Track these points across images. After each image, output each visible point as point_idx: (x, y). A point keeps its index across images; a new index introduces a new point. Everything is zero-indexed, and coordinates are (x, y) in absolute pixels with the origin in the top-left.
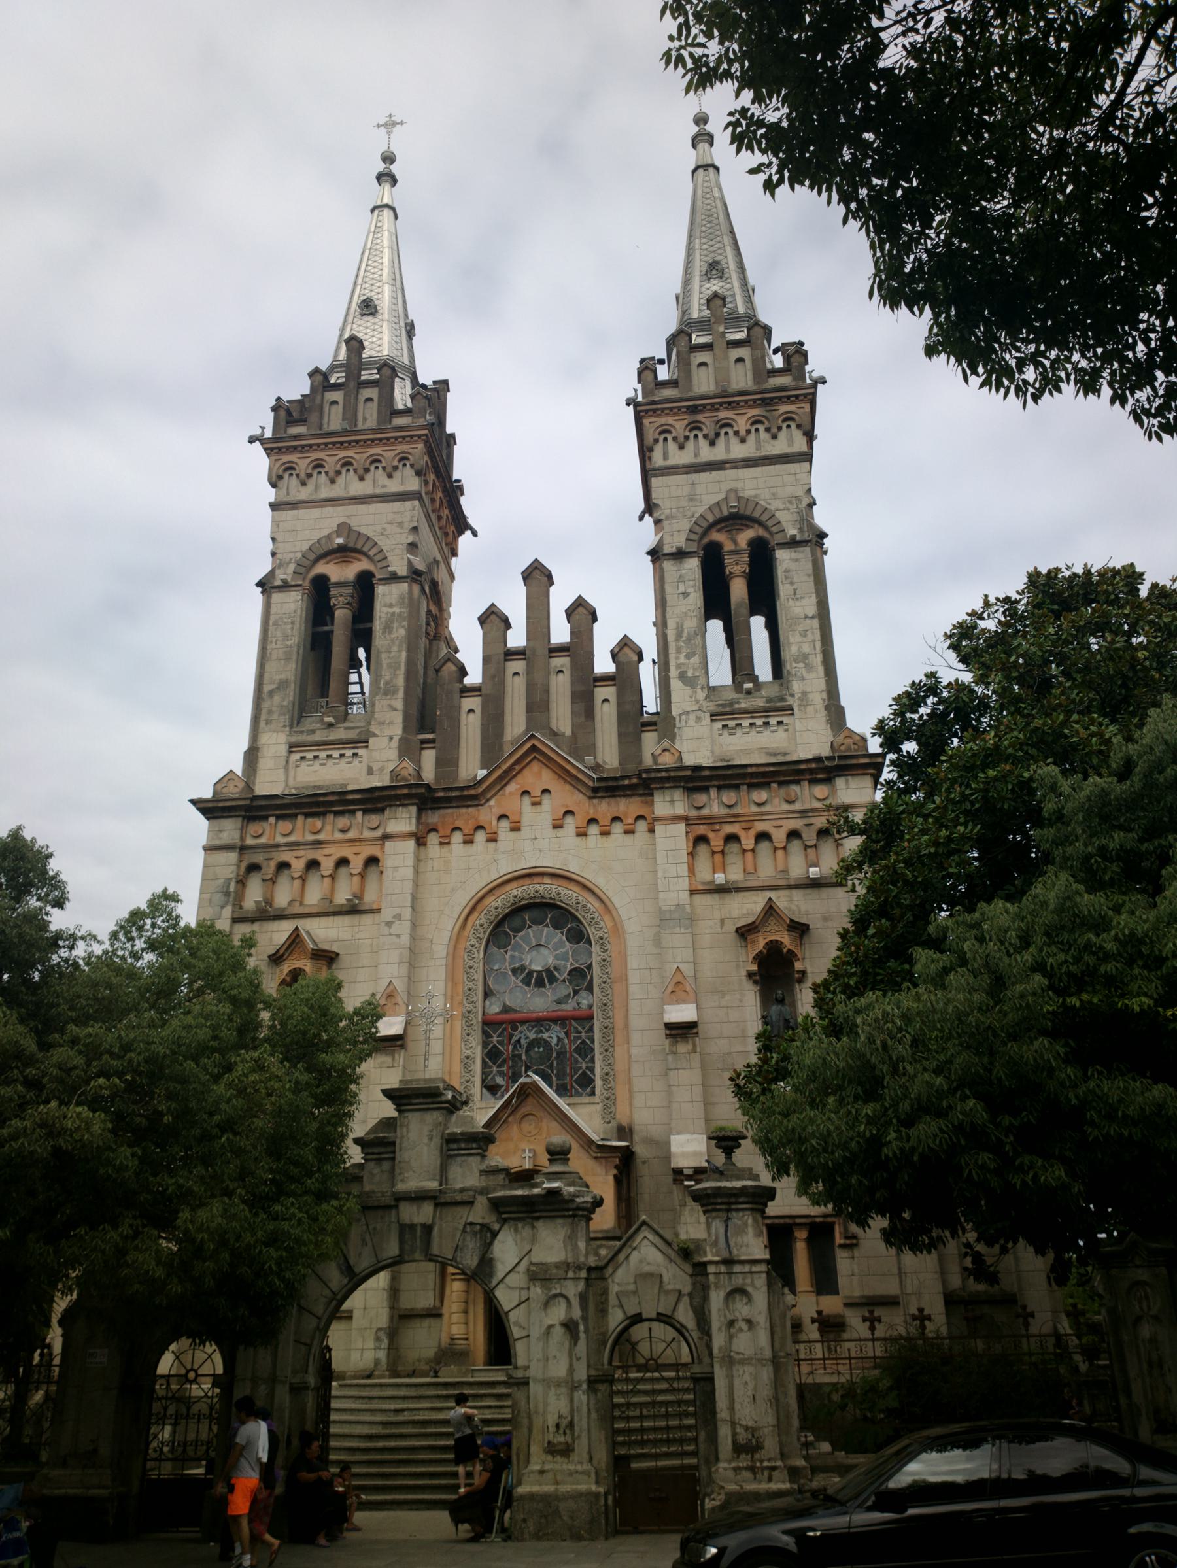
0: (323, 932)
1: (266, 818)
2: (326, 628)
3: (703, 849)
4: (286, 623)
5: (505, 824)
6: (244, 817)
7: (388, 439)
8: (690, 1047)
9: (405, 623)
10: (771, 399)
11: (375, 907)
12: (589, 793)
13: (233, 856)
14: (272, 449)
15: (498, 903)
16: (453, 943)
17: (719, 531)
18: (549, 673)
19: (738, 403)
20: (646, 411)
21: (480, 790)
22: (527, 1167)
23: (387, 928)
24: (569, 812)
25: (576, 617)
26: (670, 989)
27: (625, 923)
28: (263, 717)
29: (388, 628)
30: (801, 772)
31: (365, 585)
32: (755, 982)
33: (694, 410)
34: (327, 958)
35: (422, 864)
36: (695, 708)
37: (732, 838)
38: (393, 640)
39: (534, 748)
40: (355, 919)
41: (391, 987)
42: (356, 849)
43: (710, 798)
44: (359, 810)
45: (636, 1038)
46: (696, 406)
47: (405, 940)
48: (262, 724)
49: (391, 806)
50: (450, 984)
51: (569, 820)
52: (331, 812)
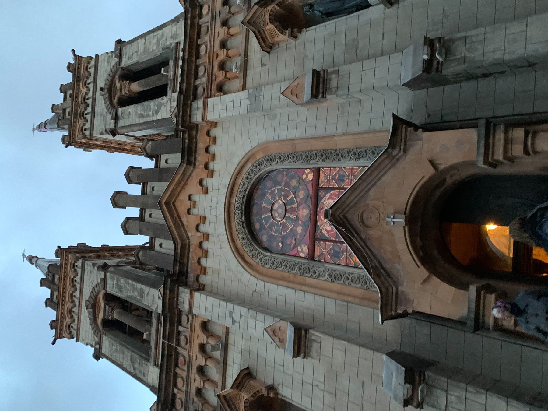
1: (174, 395)
3: (226, 88)
4: (112, 349)
5: (202, 227)
8: (334, 76)
9: (120, 278)
10: (78, 77)
11: (225, 330)
12: (191, 168)
14: (60, 334)
15: (240, 235)
16: (257, 275)
21: (179, 241)
22: (403, 221)
23: (236, 324)
24: (201, 183)
25: (133, 178)
26: (294, 98)
27: (260, 142)
28: (142, 377)
29: (120, 289)
30: (192, 25)
31: (110, 298)
32: (300, 32)
33: (76, 114)
36: (169, 102)
37: (222, 67)
39: (167, 203)
41: (269, 330)
43: (200, 84)
44: (177, 328)
45: (331, 130)
47: (244, 311)
48: (144, 379)
49: (177, 304)
50: (281, 282)
51: (205, 183)
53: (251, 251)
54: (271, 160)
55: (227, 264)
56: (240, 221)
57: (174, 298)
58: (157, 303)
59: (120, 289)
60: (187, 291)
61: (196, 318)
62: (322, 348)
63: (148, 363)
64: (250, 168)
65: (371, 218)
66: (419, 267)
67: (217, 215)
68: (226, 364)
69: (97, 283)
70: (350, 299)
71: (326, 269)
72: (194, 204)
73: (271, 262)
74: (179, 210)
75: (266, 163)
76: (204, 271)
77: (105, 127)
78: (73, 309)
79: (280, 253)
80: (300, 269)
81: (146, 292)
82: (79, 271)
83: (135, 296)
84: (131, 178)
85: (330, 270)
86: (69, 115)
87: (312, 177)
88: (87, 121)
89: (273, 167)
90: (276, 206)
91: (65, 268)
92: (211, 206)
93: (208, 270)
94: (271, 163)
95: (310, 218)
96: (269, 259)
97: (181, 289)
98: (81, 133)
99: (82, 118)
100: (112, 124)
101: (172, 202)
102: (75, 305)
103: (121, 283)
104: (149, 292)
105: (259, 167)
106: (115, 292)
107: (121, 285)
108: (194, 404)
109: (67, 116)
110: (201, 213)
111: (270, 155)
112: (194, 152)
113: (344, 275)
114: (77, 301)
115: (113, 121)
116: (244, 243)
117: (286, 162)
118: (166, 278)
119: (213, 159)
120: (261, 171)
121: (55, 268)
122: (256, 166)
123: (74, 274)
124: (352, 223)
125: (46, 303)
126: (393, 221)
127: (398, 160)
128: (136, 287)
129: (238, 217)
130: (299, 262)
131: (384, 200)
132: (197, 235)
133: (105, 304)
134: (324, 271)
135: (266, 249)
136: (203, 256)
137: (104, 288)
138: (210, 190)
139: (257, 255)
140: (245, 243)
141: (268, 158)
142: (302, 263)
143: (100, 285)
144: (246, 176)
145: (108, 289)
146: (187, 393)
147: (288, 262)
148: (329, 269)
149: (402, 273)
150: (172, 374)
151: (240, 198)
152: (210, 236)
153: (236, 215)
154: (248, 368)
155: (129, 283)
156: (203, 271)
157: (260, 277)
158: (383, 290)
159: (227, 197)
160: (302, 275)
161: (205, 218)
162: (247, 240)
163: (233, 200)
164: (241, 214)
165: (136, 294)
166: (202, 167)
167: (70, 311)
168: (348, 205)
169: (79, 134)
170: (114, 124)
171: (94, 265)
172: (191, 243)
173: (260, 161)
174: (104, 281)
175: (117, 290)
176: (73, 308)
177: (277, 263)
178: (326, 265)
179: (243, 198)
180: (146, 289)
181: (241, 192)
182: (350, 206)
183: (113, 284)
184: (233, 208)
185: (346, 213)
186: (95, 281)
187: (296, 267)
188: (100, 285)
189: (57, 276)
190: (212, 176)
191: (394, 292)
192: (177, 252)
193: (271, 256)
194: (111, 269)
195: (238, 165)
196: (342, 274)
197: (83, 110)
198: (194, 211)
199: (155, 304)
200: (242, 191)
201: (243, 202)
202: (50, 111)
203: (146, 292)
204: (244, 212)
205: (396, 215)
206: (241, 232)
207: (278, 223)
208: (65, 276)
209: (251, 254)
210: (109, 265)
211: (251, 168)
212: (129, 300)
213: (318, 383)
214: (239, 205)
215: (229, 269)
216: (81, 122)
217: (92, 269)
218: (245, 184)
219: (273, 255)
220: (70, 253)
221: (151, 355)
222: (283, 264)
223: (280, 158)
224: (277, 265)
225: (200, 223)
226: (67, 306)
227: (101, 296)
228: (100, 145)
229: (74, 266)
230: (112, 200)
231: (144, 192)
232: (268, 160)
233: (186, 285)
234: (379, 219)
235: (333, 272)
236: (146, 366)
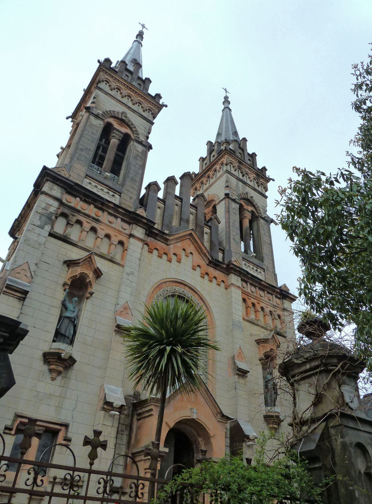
0: (100, 263)
7: (147, 100)
13: (56, 204)
17: (243, 201)
19: (252, 170)
27: (216, 320)
34: (98, 273)
42: (116, 234)
44: (120, 217)
46: (241, 162)
127: (216, 417)
150: (90, 201)
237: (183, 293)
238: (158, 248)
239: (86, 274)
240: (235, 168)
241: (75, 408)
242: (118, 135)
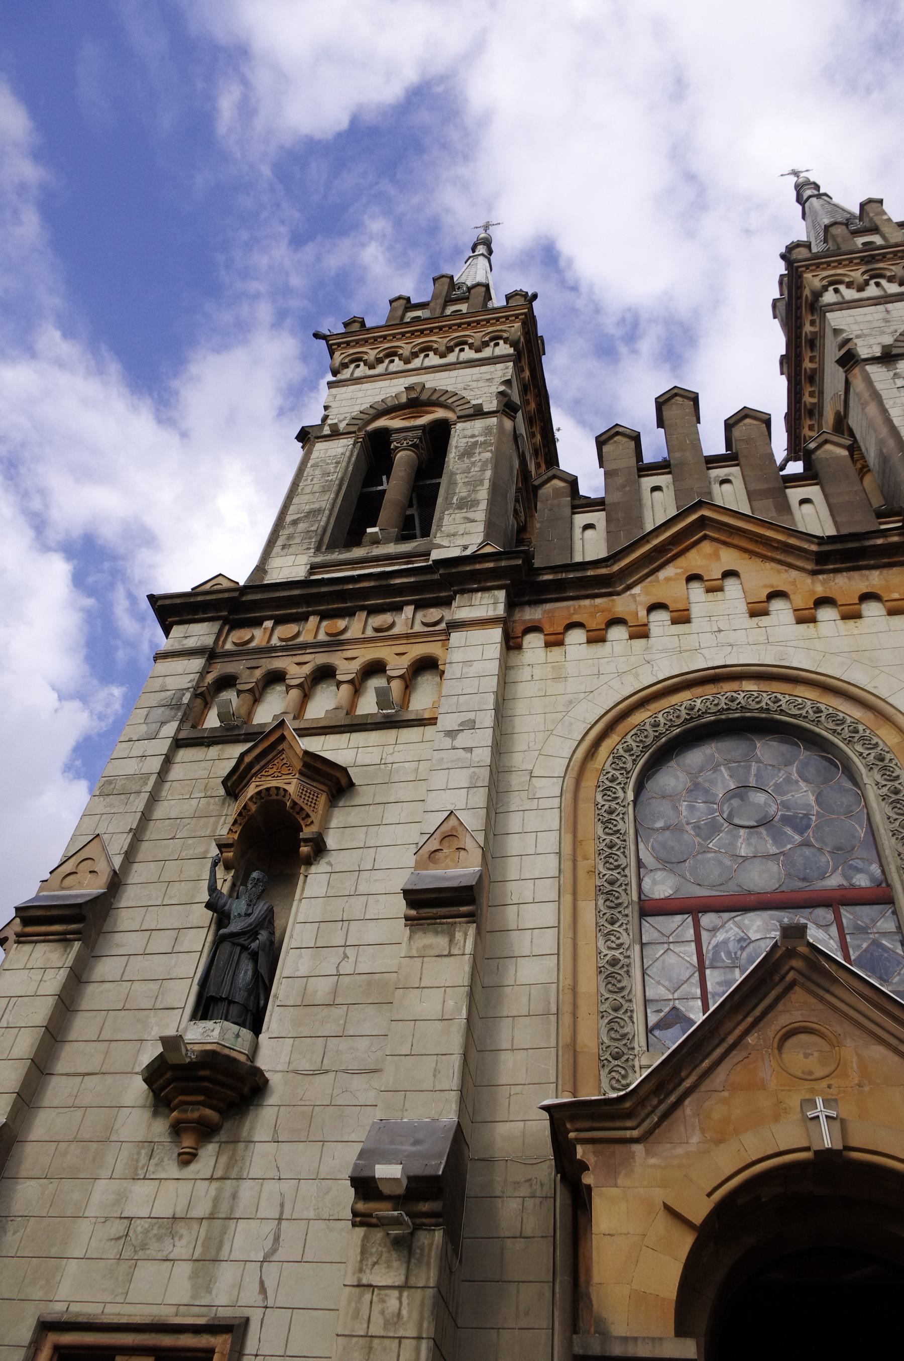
1: (258, 623)
2: (380, 488)
4: (328, 464)
6: (225, 621)
11: (427, 715)
16: (572, 774)
18: (710, 483)
20: (807, 267)
21: (616, 568)
22: (828, 1144)
28: (280, 542)
33: (872, 259)
35: (512, 673)
38: (474, 463)
39: (703, 522)
40: (389, 735)
41: (452, 822)
44: (408, 603)
47: (484, 755)
48: (277, 549)
49: (463, 592)
50: (568, 839)
51: (777, 605)
52: (362, 608)
53: (629, 750)
54: (884, 768)
55: (583, 695)
56: (699, 709)
57: (479, 582)
58: (452, 545)
59: (468, 453)
60: (500, 610)
61: (440, 643)
62: (437, 958)
63: (312, 551)
64: (847, 717)
65: (806, 1056)
66: (709, 1195)
67: (703, 651)
68: (351, 732)
69: (468, 398)
70: (567, 1019)
71: (627, 949)
72: (714, 589)
73: (613, 805)
74: (692, 555)
75: (873, 755)
76: (555, 642)
77: (858, 337)
78: (396, 359)
79: (638, 826)
80: (612, 883)
81: (471, 515)
82: (487, 352)
83: (457, 491)
84: (741, 424)
85: (626, 960)
86: (863, 244)
87: (863, 884)
88: (861, 289)
89: (864, 776)
90: (760, 798)
91: (488, 321)
92: (720, 631)
93: (556, 651)
94: (876, 770)
95: (750, 893)
96: (620, 801)
97: (501, 595)
98: (825, 283)
99: (866, 277)
100: (869, 351)
101: (708, 533)
102: (407, 362)
103: (480, 453)
104: (474, 521)
105: (856, 739)
106: (457, 442)
107: (477, 454)
108: (248, 671)
109: (860, 241)
110: (696, 611)
111: (896, 765)
112: (855, 564)
113: (623, 997)
114: (416, 363)
115: (877, 352)
116: (646, 730)
117: (888, 810)
118: (522, 555)
119: (845, 617)
120: (847, 744)
121: (481, 299)
122: (857, 732)
123: (477, 343)
124: (780, 1007)
125: (400, 298)
126: (818, 1117)
128: (478, 488)
129: (708, 703)
130: (629, 879)
131: (867, 1089)
132: (639, 608)
133: (423, 427)
134: (622, 944)
135: (639, 788)
136: (591, 633)
137: (458, 417)
138: (763, 621)
139: (622, 768)
140: (646, 733)
141: (887, 761)
142: (628, 888)
143: (467, 406)
144: (823, 707)
145: (459, 426)
146: (268, 651)
147: (622, 850)
148: (629, 957)
149: (680, 1150)
151: (758, 703)
152: (643, 641)
153: (712, 699)
154: (351, 784)
155: (483, 470)
156: (552, 638)
157: (570, 783)
158: (628, 1105)
159: (740, 668)
160: (599, 890)
161: (687, 620)
162: (656, 736)
163: (749, 686)
164: (719, 711)
165: (461, 491)
166: (820, 590)
167: (392, 354)
168: (828, 991)
169: (823, 278)
170: (869, 356)
171: (508, 383)
172: (615, 597)
173: (875, 740)
174: (478, 413)
175: (461, 449)
176: (400, 359)
177: (615, 823)
178: (637, 948)
179: (761, 710)
180: (480, 514)
181: (777, 701)
182: (828, 997)
183: (473, 436)
184: (728, 687)
185: (802, 986)
186: (472, 393)
187: (615, 873)
188: (467, 406)
189: (464, 307)
190: (800, 621)
191: (628, 1134)
192: (587, 569)
193: (629, 804)
194: (508, 424)
195: (849, 683)
196: (625, 993)
197: (889, 274)
198: (697, 591)
199: (450, 541)
200: (781, 703)
201: (751, 710)
202: (863, 198)
203: (471, 515)
204: (723, 717)
205: (837, 1125)
206: (671, 717)
207: (714, 811)
208: (469, 324)
209: (621, 752)
210: (515, 418)
211: (849, 720)
212: (444, 481)
213: (352, 959)
214: (740, 703)
215: (571, 702)
216: (857, 275)
217: (498, 380)
218: (799, 709)
219: (631, 808)
220: (524, 324)
221: (333, 553)
222: (614, 838)
223: (896, 792)
224: (609, 821)
225: (672, 612)
226: (403, 345)
227: (440, 413)
228: (801, 333)
229: (495, 339)
230: (676, 391)
231: (713, 461)
232: (882, 759)
233: (511, 605)
234: (808, 1078)
235: (625, 969)
236: (305, 547)
237: (734, 705)
238: (576, 618)
239: (278, 788)
240: (855, 286)
241: (274, 1250)
242: (405, 439)
